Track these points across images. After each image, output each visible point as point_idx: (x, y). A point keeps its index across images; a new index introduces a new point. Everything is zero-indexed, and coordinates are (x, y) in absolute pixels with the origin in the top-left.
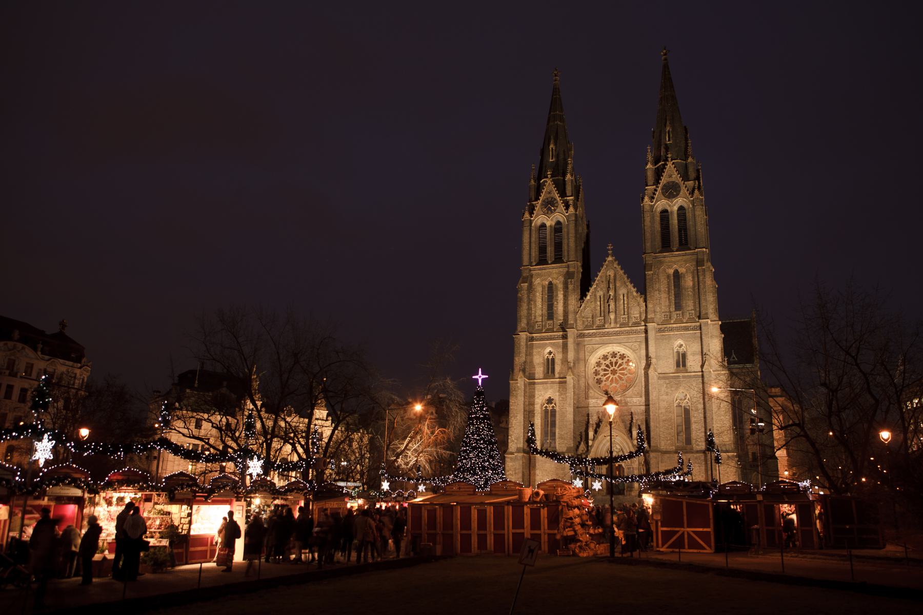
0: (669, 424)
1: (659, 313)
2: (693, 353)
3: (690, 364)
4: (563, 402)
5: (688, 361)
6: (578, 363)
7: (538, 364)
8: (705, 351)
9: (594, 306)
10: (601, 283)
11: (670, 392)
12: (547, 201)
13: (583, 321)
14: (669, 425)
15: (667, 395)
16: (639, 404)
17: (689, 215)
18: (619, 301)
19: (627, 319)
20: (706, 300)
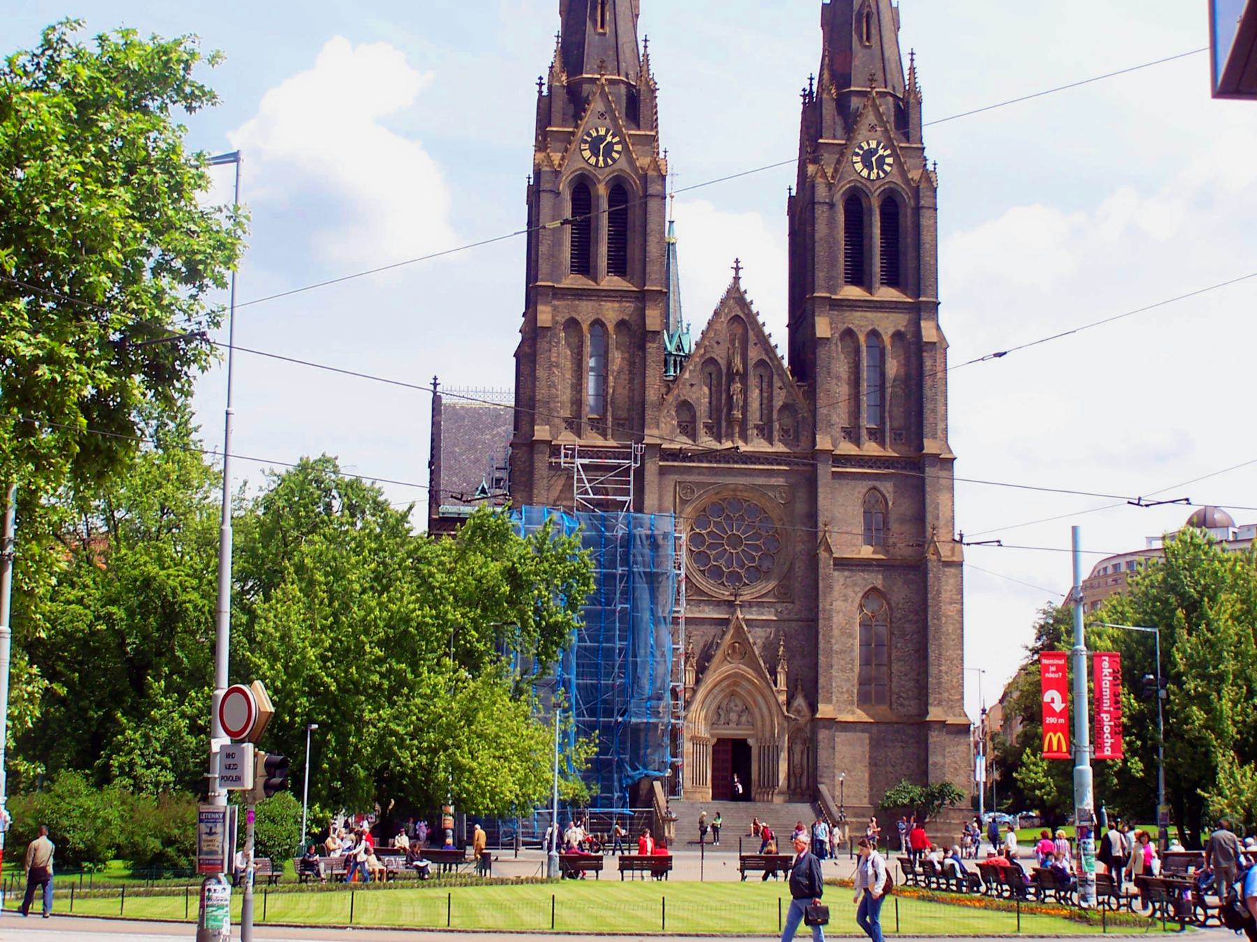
8: (929, 518)
10: (715, 345)
11: (853, 595)
12: (594, 134)
15: (844, 601)
17: (906, 221)
20: (934, 411)
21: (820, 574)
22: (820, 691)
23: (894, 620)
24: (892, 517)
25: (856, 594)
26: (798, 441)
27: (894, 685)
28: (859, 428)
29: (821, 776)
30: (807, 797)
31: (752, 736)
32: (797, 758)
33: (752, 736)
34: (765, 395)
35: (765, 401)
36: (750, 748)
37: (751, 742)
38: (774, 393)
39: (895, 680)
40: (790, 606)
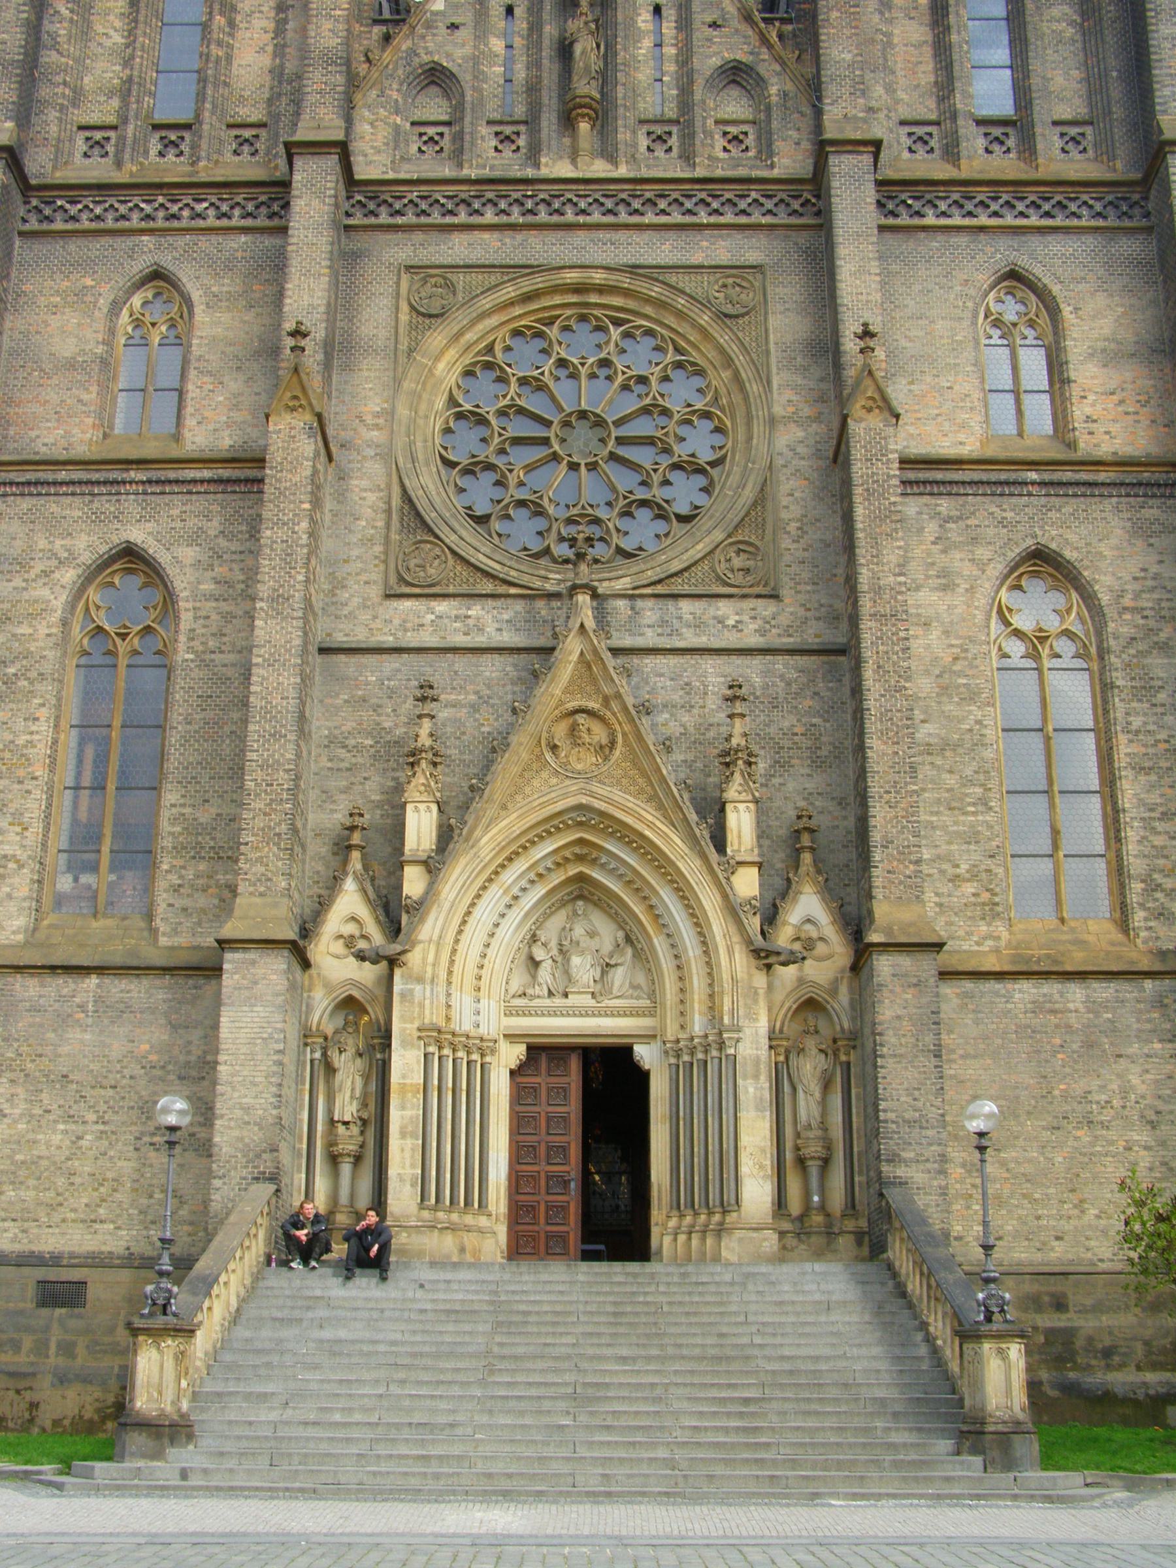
0: (969, 772)
1: (881, 115)
2: (1104, 350)
3: (1088, 410)
4: (225, 607)
5: (1075, 391)
6: (347, 368)
7: (71, 365)
9: (468, 50)
11: (968, 569)
13: (397, 129)
14: (968, 782)
15: (945, 588)
16: (754, 641)
18: (635, 37)
19: (674, 141)
21: (857, 479)
22: (877, 855)
23: (1112, 642)
24: (1076, 348)
25: (982, 566)
26: (771, 155)
27: (1132, 847)
28: (954, 116)
29: (894, 1159)
30: (845, 1242)
31: (649, 1038)
32: (807, 1107)
33: (649, 1038)
34: (670, 51)
35: (671, 67)
36: (642, 1078)
37: (645, 1054)
38: (697, 35)
39: (1132, 835)
40: (767, 608)
